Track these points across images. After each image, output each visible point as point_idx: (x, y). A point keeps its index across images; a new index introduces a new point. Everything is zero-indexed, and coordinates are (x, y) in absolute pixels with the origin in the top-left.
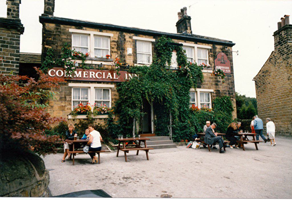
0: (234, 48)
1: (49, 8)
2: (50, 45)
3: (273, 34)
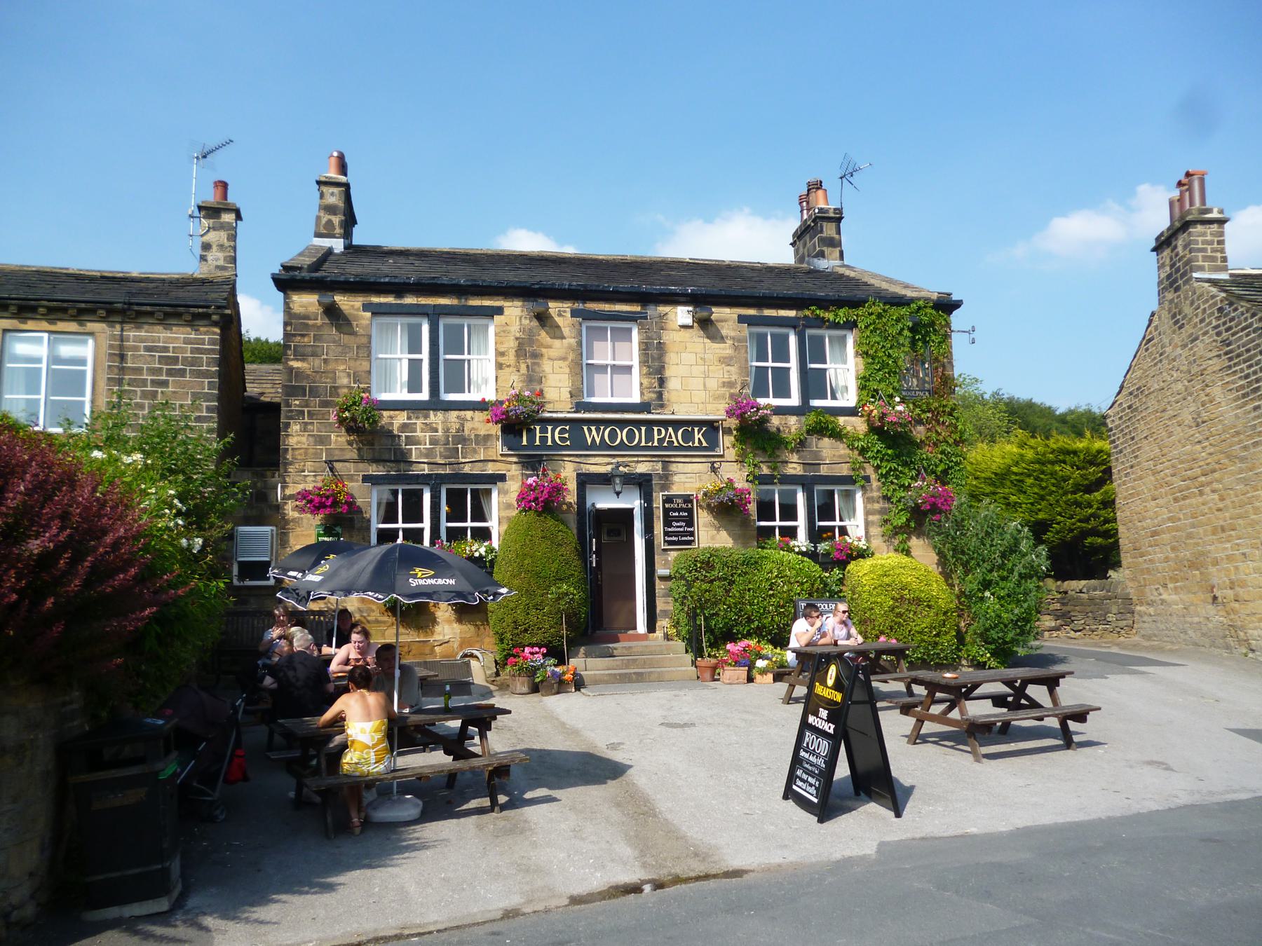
0: (957, 319)
1: (330, 221)
2: (303, 360)
3: (1153, 244)
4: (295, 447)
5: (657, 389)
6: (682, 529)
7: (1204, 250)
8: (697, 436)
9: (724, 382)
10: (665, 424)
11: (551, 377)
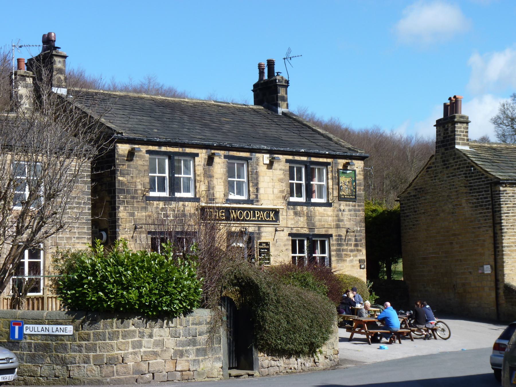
2: (124, 177)
3: (435, 124)
4: (122, 217)
5: (256, 193)
7: (460, 135)
8: (272, 215)
9: (280, 191)
10: (260, 210)
11: (217, 187)
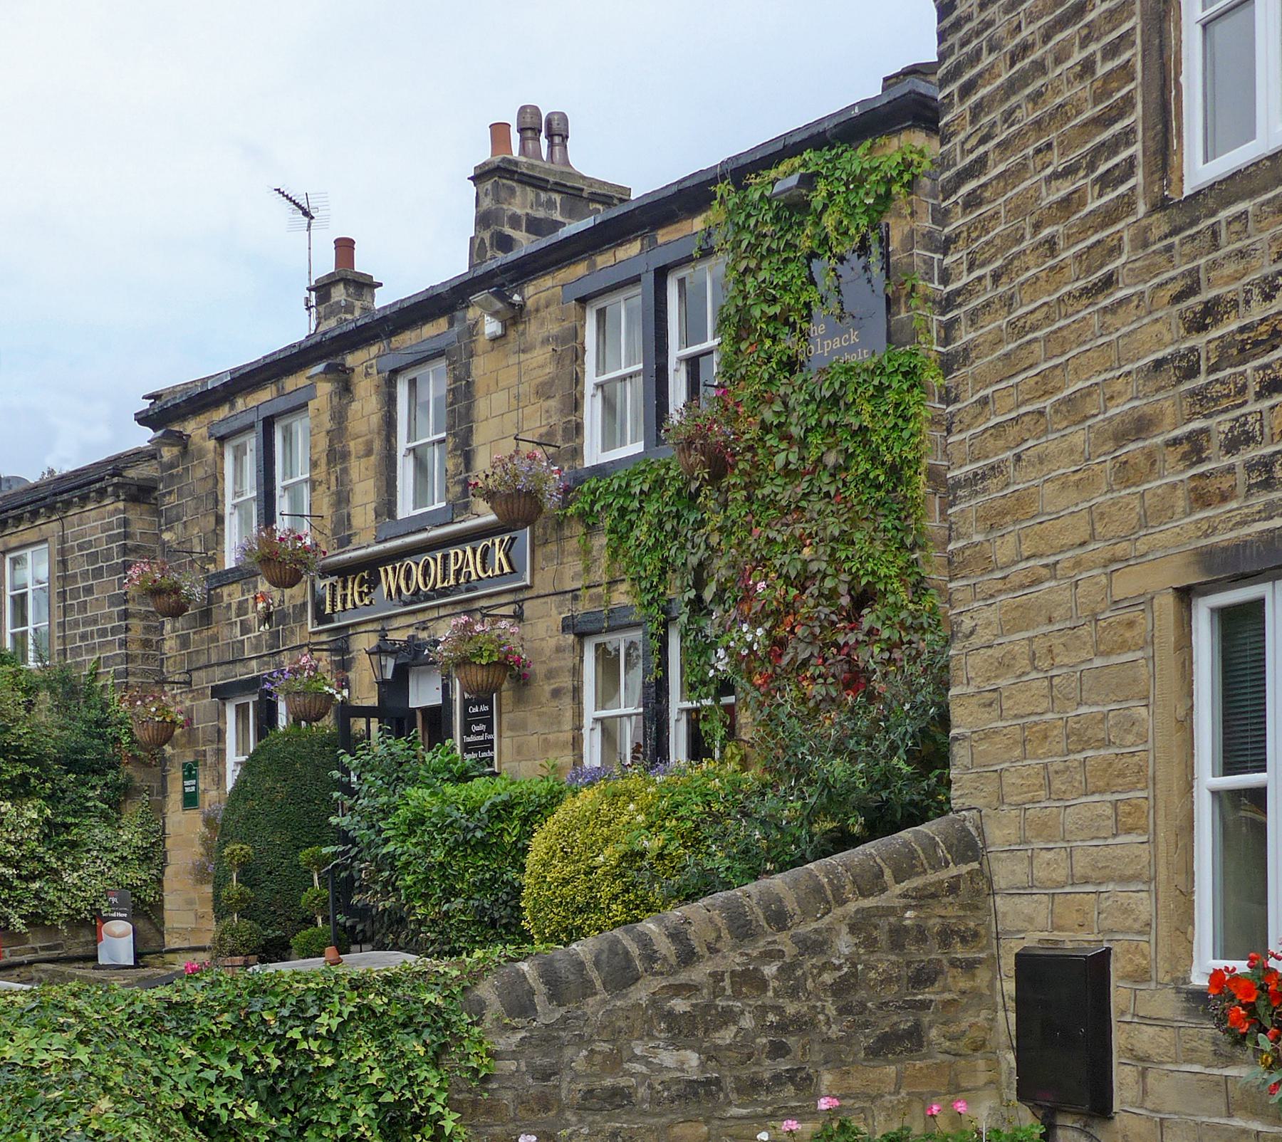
6: (481, 738)
